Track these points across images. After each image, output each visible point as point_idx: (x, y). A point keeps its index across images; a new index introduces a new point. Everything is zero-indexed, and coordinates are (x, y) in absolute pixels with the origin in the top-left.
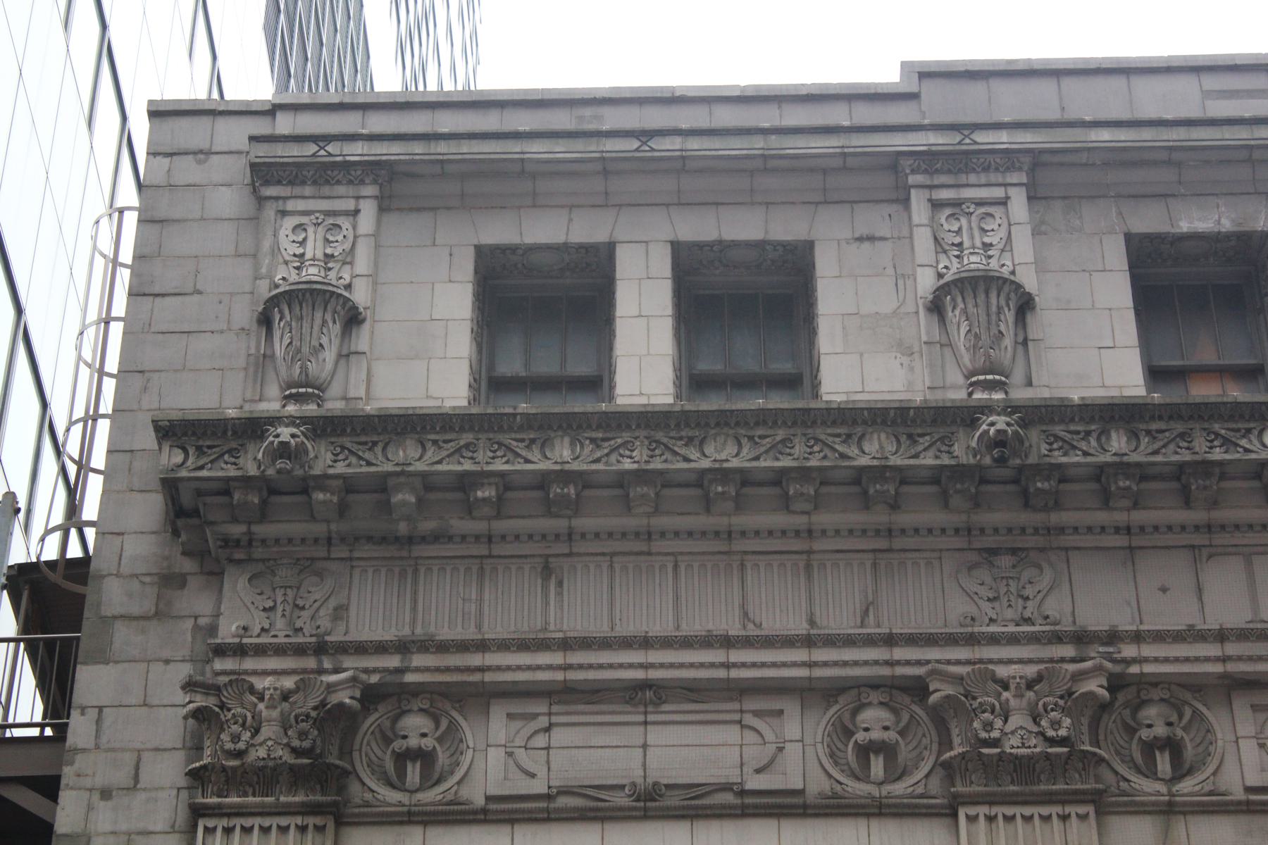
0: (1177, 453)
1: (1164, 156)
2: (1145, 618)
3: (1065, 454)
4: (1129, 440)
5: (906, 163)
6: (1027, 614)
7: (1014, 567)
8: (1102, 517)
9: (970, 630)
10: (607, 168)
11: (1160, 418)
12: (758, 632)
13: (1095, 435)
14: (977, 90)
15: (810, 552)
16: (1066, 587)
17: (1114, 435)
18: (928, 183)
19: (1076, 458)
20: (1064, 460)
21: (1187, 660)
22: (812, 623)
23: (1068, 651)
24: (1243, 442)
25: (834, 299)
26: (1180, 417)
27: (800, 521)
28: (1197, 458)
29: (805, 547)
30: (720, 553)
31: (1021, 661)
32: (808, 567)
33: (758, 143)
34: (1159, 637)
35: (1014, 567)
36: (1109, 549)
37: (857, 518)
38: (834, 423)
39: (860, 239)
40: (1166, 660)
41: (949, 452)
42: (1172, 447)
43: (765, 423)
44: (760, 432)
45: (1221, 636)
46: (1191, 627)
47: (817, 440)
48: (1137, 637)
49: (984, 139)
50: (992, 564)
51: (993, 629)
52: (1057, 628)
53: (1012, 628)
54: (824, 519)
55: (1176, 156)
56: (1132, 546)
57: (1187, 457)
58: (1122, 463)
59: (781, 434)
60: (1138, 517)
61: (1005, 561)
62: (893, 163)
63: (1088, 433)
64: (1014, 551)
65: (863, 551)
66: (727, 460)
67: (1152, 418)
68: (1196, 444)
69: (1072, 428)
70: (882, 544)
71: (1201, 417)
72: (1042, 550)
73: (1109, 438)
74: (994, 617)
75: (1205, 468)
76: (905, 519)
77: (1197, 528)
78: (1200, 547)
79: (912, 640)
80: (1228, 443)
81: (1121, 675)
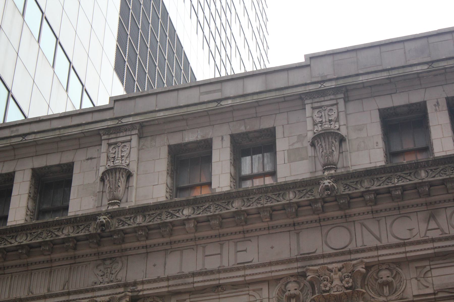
0: (156, 221)
1: (181, 118)
2: (147, 276)
3: (123, 226)
4: (143, 218)
5: (101, 132)
6: (112, 279)
7: (110, 264)
8: (137, 244)
9: (92, 287)
10: (14, 147)
11: (153, 210)
12: (32, 296)
13: (133, 218)
14: (132, 102)
15: (52, 267)
16: (125, 269)
17: (138, 217)
18: (108, 138)
19: (126, 227)
20: (122, 228)
21: (157, 288)
22: (49, 290)
23: (121, 290)
24: (177, 214)
25: (77, 180)
26: (159, 209)
27: (48, 257)
28: (162, 221)
29: (50, 266)
30: (25, 271)
31: (104, 296)
32: (51, 272)
33: (57, 132)
34: (149, 282)
35: (110, 264)
36: (140, 254)
37: (64, 254)
38: (55, 225)
39: (88, 159)
40: (151, 289)
41: (88, 230)
42: (156, 219)
43: (35, 228)
44: (34, 231)
45: (168, 279)
46: (159, 277)
47: (50, 231)
48: (143, 283)
49: (125, 121)
50: (104, 264)
51: (102, 285)
52: (119, 283)
53: (106, 285)
54: (55, 256)
55: (185, 117)
56: (147, 251)
57: (159, 221)
58: (139, 226)
59: (40, 231)
60: (149, 242)
61: (108, 262)
62: (98, 133)
63: (131, 218)
64: (111, 259)
65: (47, 268)
66: (22, 242)
67: (151, 210)
68: (162, 217)
69: (126, 217)
70: (72, 261)
71: (165, 208)
72: (120, 257)
73: (137, 219)
74: (102, 281)
75: (165, 224)
76: (79, 253)
77: (167, 243)
78: (168, 250)
79: (76, 292)
80: (172, 215)
81: (137, 296)
